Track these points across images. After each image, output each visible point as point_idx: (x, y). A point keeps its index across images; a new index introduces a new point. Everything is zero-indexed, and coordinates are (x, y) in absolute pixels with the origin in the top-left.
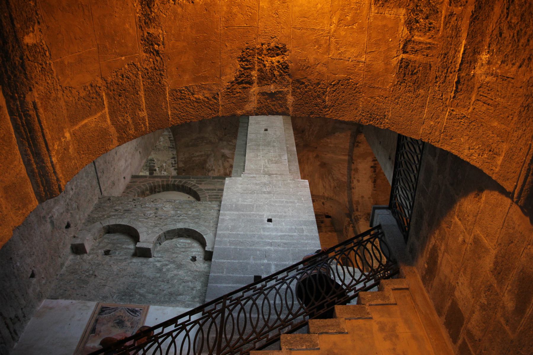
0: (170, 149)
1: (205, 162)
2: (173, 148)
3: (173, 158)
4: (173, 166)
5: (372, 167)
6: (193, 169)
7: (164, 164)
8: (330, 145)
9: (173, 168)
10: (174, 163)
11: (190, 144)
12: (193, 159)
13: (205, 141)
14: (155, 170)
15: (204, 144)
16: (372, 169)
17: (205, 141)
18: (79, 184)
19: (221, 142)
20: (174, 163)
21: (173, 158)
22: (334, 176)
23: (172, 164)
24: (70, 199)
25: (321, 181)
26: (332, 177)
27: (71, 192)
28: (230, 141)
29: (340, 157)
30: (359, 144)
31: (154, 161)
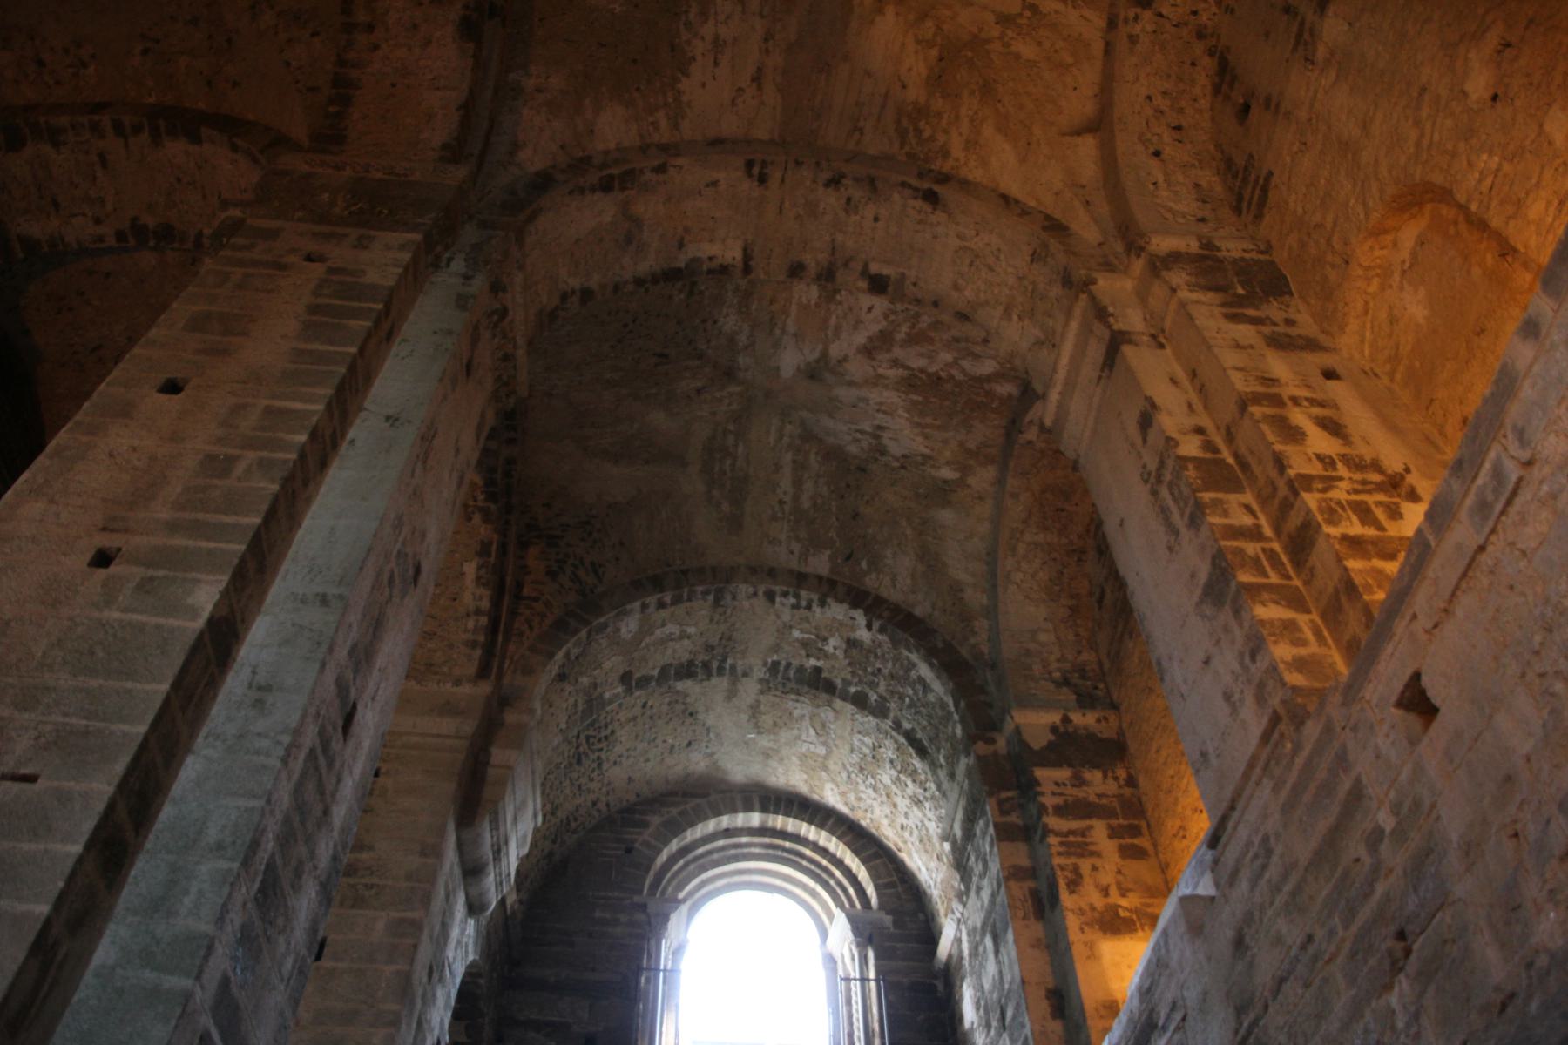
1: (833, 454)
3: (770, 596)
4: (809, 607)
6: (856, 516)
7: (796, 634)
9: (816, 609)
10: (793, 600)
11: (726, 507)
12: (806, 503)
13: (731, 440)
14: (818, 670)
15: (740, 449)
17: (731, 440)
20: (793, 600)
21: (770, 596)
23: (796, 607)
28: (732, 340)
31: (776, 664)
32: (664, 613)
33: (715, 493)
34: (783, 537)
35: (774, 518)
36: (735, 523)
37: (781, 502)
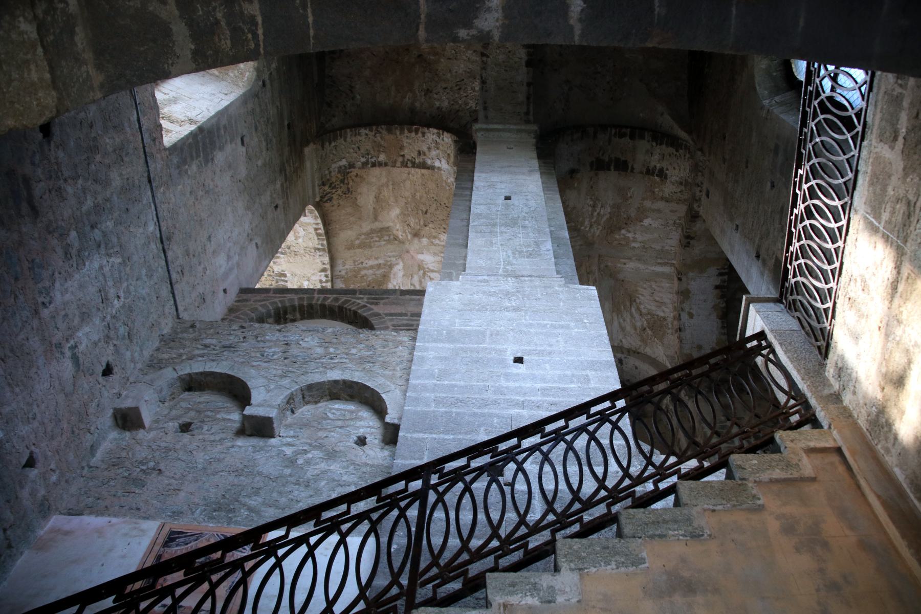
0: (318, 253)
2: (324, 250)
3: (324, 270)
5: (717, 287)
8: (634, 245)
10: (324, 280)
11: (357, 242)
12: (363, 273)
13: (386, 238)
16: (717, 291)
17: (386, 238)
18: (132, 288)
19: (416, 241)
20: (324, 280)
21: (324, 270)
22: (642, 307)
24: (113, 317)
25: (615, 318)
26: (638, 309)
27: (116, 302)
28: (435, 237)
29: (653, 268)
30: (692, 242)
31: (285, 276)
32: (312, 231)
33: (363, 237)
34: (347, 267)
35: (355, 261)
36: (351, 247)
37: (362, 263)
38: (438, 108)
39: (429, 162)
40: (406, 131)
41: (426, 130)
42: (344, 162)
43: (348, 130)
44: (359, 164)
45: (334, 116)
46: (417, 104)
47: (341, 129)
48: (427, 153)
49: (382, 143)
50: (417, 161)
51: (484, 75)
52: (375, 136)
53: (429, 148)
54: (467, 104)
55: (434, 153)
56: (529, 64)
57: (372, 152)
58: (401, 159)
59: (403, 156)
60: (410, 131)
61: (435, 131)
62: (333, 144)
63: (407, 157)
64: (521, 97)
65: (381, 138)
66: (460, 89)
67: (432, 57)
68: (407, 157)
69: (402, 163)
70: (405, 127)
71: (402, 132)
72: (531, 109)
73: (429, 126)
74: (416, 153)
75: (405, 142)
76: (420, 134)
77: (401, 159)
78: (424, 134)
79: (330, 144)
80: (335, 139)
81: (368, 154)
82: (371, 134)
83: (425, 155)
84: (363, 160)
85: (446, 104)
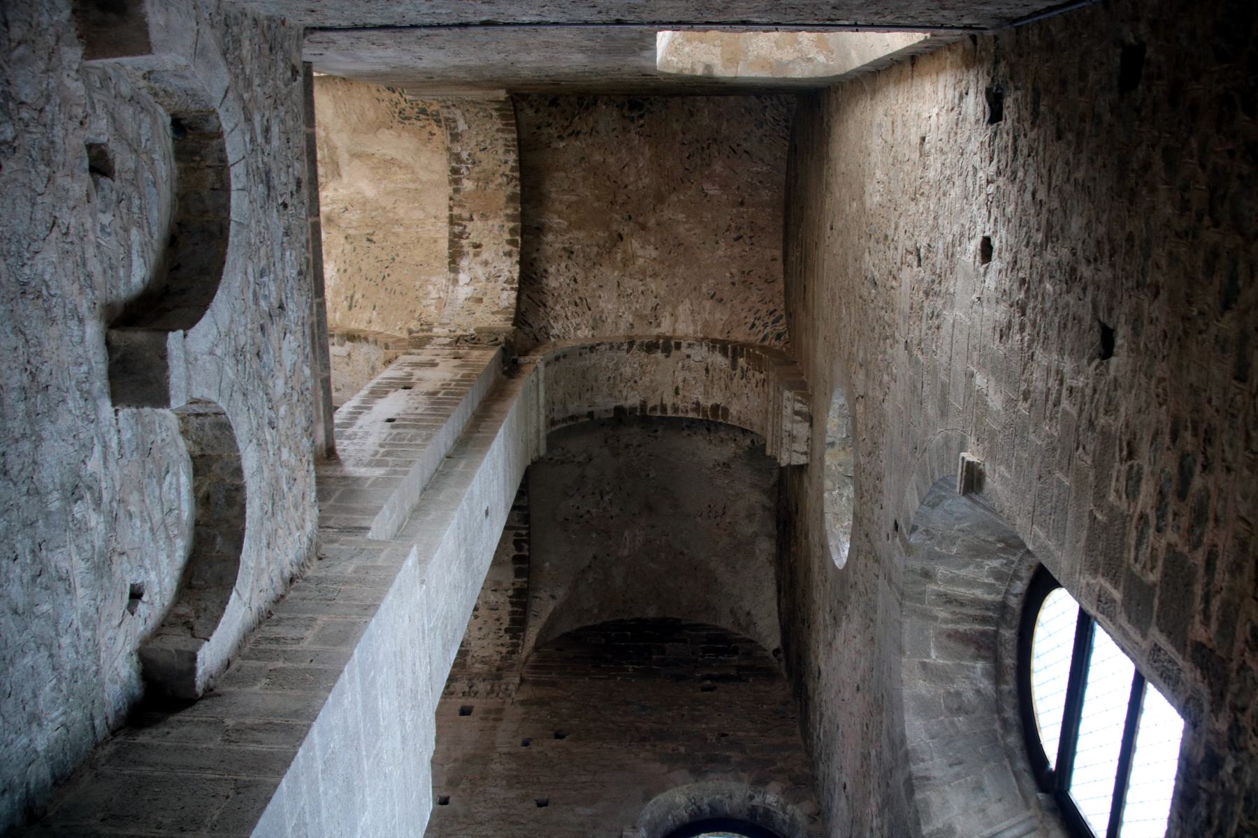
38: (546, 271)
39: (464, 263)
40: (511, 225)
41: (516, 258)
42: (462, 126)
43: (515, 136)
44: (457, 148)
45: (537, 112)
46: (550, 237)
47: (518, 125)
48: (478, 259)
49: (492, 186)
50: (464, 242)
51: (603, 347)
52: (503, 175)
53: (486, 263)
54: (556, 318)
55: (480, 271)
56: (619, 410)
57: (477, 169)
58: (466, 215)
59: (471, 219)
60: (512, 231)
61: (516, 276)
62: (495, 114)
63: (470, 226)
64: (573, 408)
65: (500, 185)
66: (576, 305)
67: (619, 256)
68: (470, 226)
69: (460, 217)
70: (518, 224)
71: (510, 218)
72: (558, 427)
73: (521, 263)
74: (477, 241)
75: (495, 223)
76: (508, 248)
77: (466, 215)
78: (509, 254)
79: (496, 110)
80: (503, 117)
81: (474, 163)
82: (506, 169)
83: (476, 255)
84: (464, 155)
85: (553, 283)
